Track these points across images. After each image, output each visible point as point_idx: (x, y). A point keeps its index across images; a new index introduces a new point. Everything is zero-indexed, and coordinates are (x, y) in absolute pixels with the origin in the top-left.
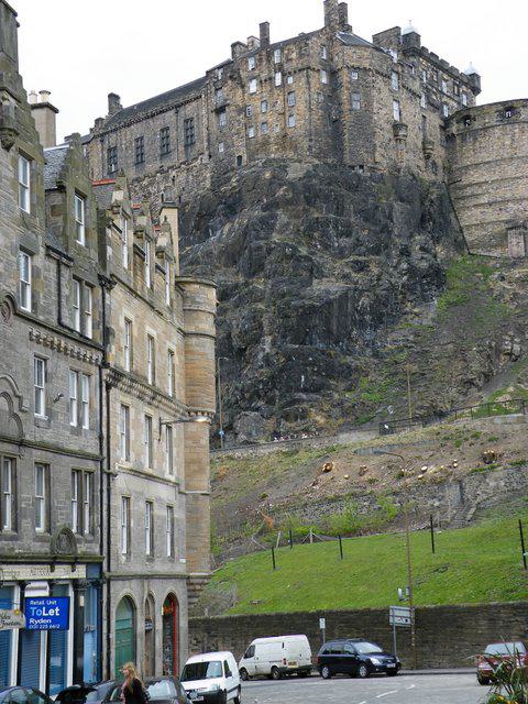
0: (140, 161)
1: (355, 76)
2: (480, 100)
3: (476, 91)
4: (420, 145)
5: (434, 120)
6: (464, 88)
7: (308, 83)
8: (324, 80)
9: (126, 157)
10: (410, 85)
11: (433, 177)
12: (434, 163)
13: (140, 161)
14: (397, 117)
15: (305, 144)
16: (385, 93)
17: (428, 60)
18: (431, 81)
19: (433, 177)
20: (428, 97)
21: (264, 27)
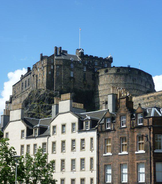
0: (26, 87)
1: (58, 67)
2: (112, 65)
3: (112, 62)
4: (82, 81)
5: (91, 73)
6: (106, 62)
7: (47, 69)
8: (52, 68)
9: (24, 84)
10: (78, 65)
11: (88, 89)
12: (89, 86)
13: (26, 87)
14: (72, 76)
15: (45, 85)
16: (67, 69)
17: (86, 57)
18: (89, 63)
19: (88, 89)
20: (87, 69)
21: (42, 54)
